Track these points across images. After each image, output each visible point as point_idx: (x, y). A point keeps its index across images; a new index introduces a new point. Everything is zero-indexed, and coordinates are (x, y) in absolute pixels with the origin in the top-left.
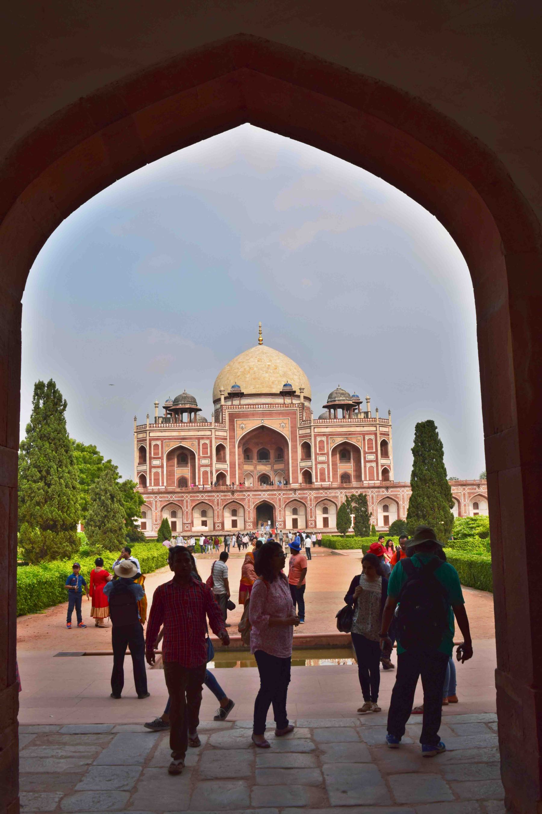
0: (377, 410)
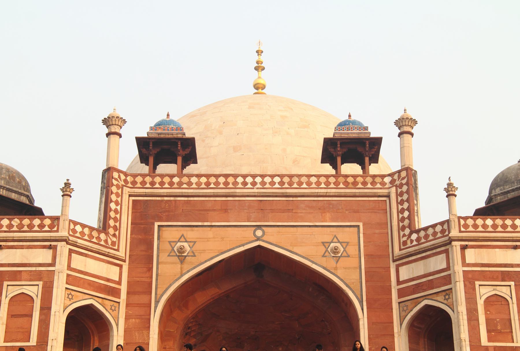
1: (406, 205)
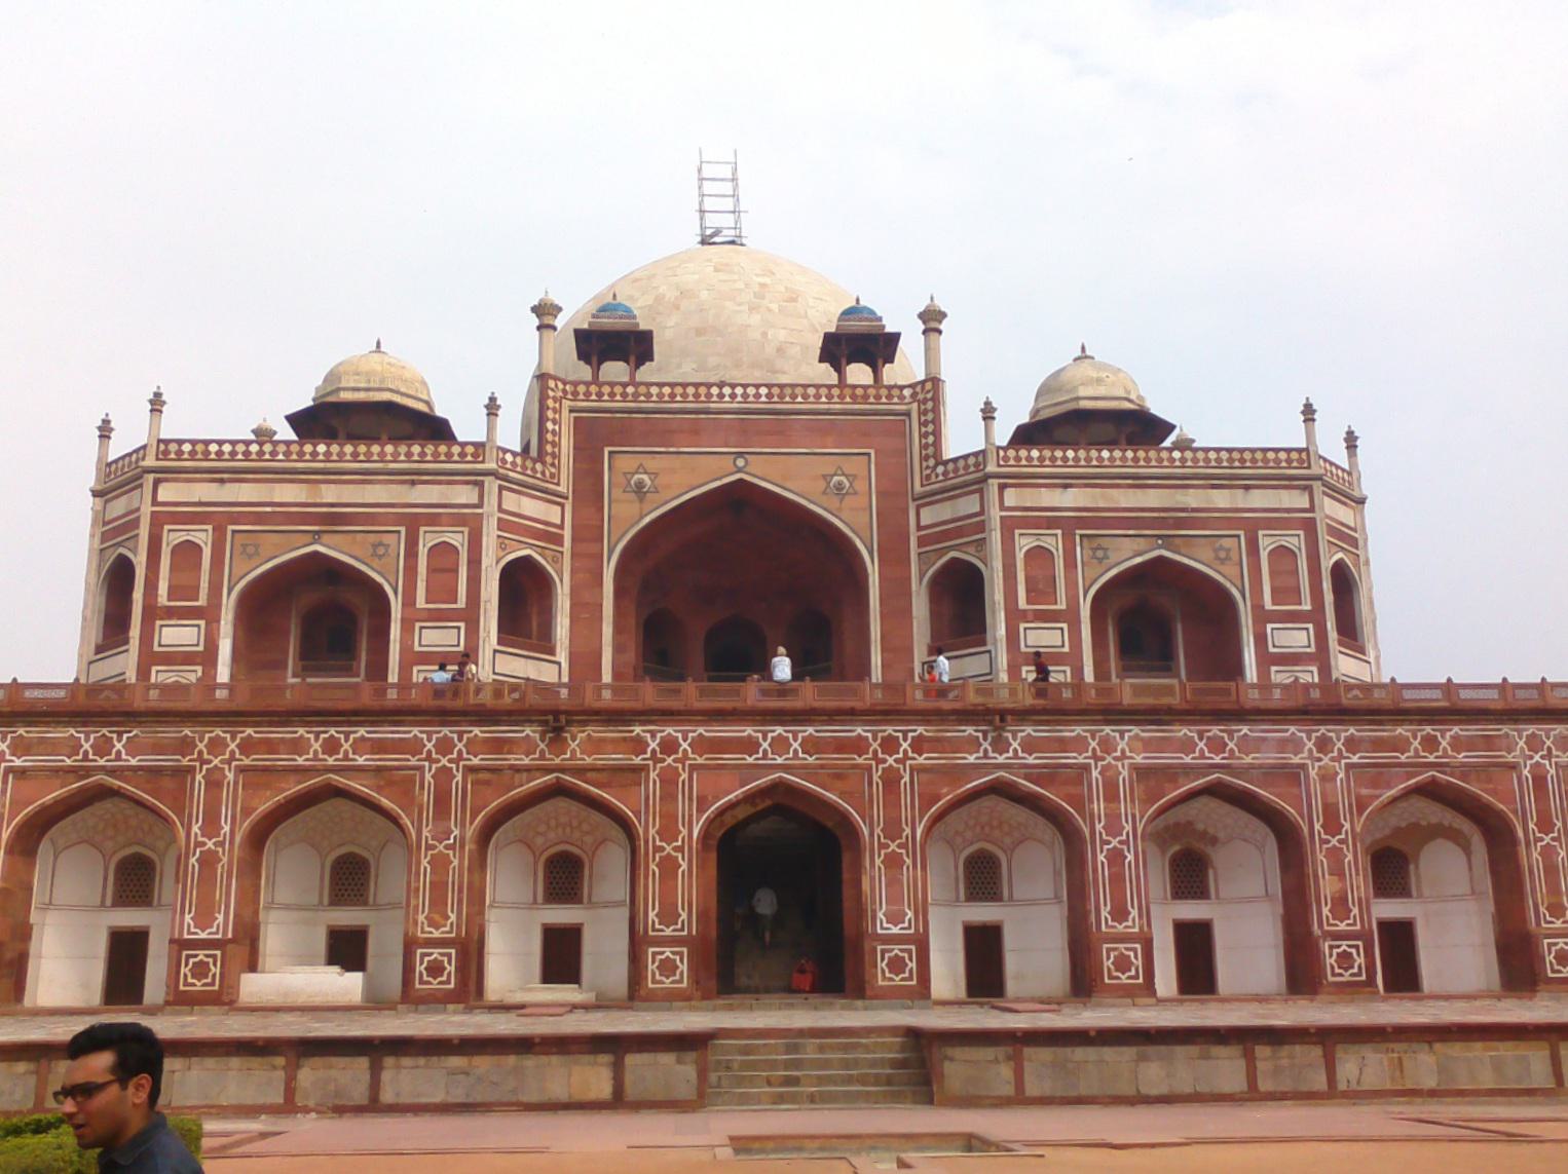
0: (1309, 412)
1: (930, 428)
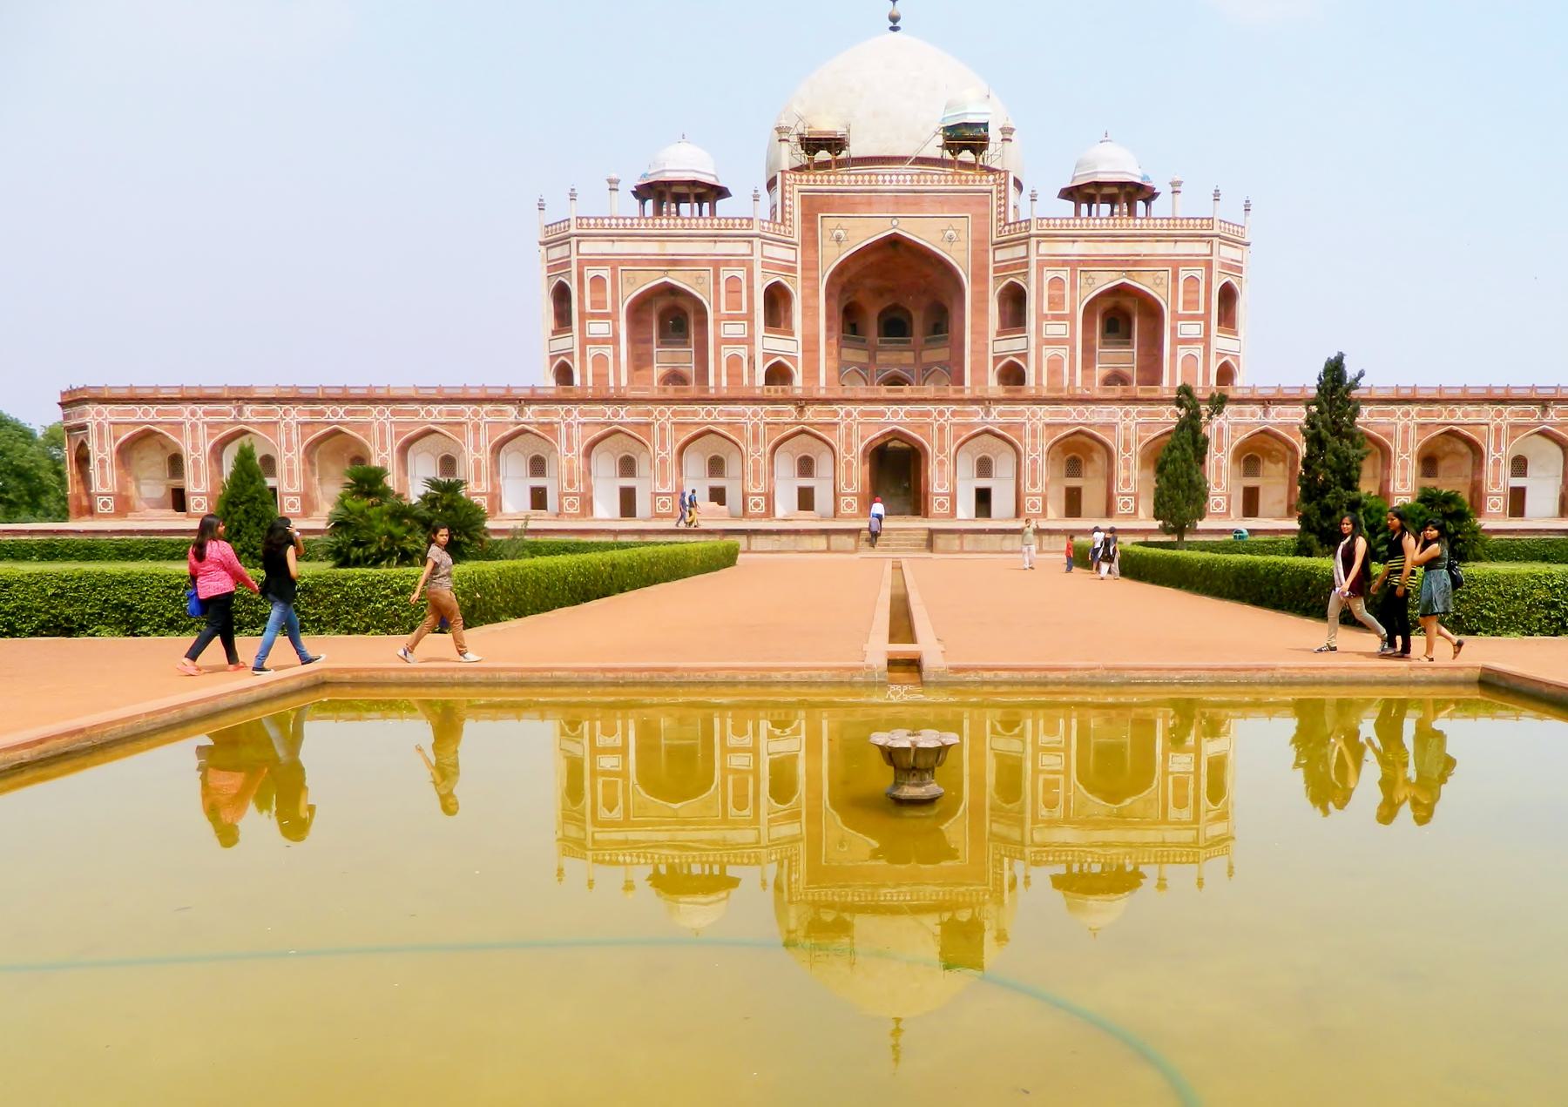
0: (1217, 196)
